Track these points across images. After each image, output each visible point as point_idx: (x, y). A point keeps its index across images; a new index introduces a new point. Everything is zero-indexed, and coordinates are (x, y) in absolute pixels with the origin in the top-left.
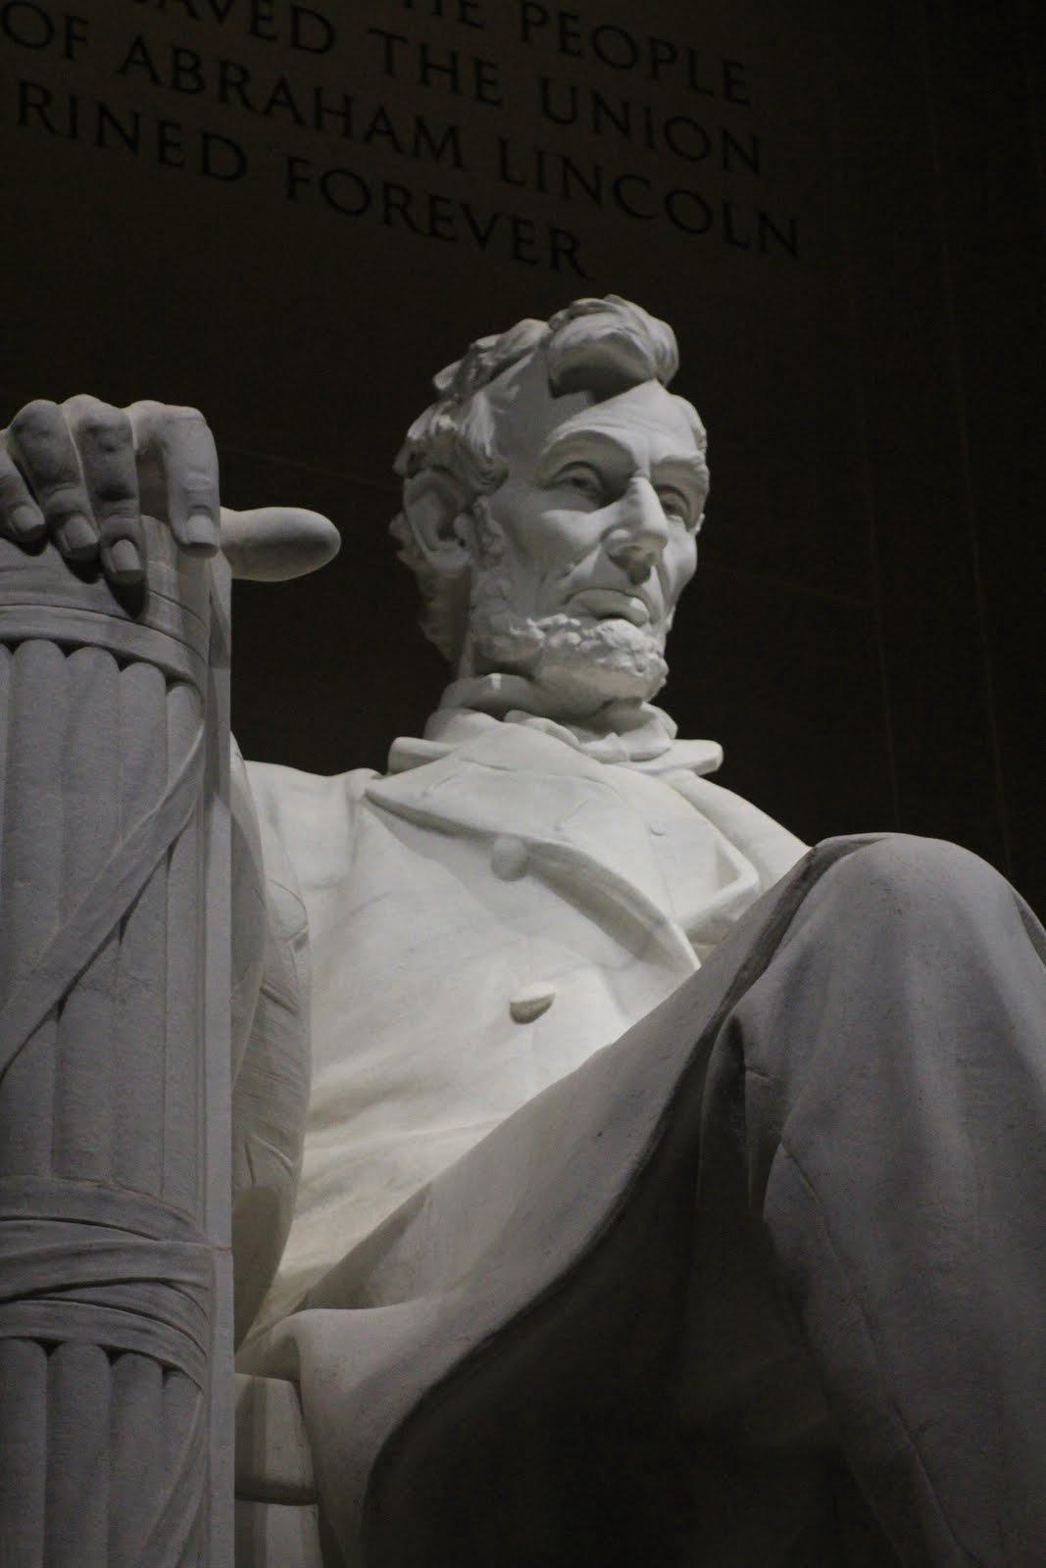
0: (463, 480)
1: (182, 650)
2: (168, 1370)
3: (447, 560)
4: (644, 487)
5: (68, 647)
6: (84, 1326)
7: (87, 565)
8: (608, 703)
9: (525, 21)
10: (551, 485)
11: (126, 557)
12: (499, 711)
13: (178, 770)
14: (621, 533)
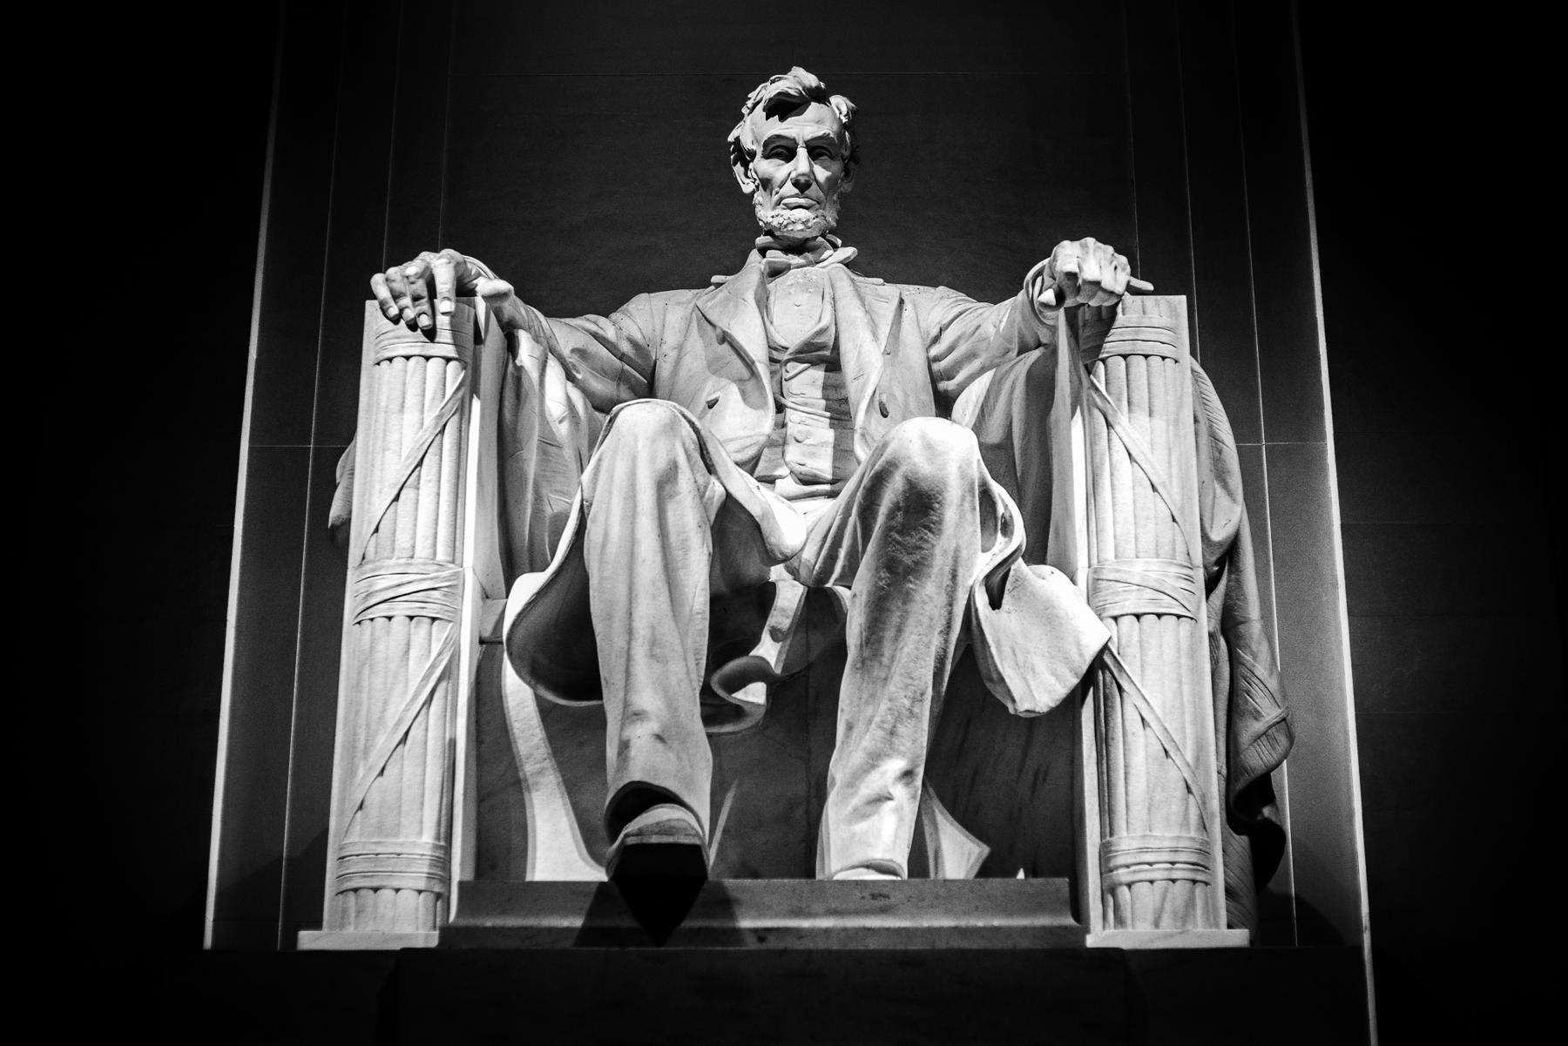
0: (745, 157)
1: (452, 348)
2: (434, 619)
3: (747, 187)
4: (802, 153)
5: (408, 358)
6: (400, 609)
7: (413, 326)
8: (807, 240)
10: (767, 156)
11: (424, 321)
12: (763, 252)
13: (449, 393)
14: (793, 175)
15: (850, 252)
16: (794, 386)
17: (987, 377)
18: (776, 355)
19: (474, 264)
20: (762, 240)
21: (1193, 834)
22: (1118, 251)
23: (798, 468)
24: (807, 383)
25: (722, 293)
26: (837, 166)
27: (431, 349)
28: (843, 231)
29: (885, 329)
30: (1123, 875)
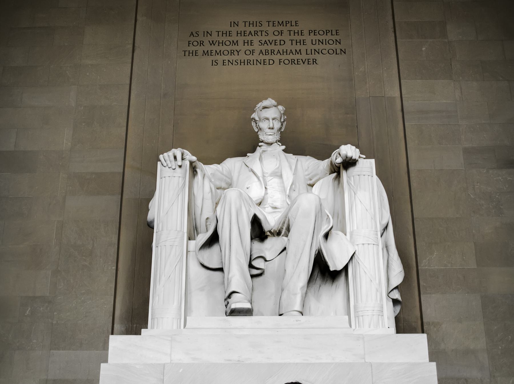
9: (310, 33)
11: (174, 168)
15: (284, 147)
16: (269, 183)
17: (321, 181)
18: (265, 175)
19: (186, 151)
20: (260, 144)
21: (379, 302)
22: (356, 148)
23: (271, 205)
24: (273, 183)
25: (250, 159)
26: (280, 124)
27: (175, 175)
28: (282, 141)
29: (293, 167)
30: (360, 314)
